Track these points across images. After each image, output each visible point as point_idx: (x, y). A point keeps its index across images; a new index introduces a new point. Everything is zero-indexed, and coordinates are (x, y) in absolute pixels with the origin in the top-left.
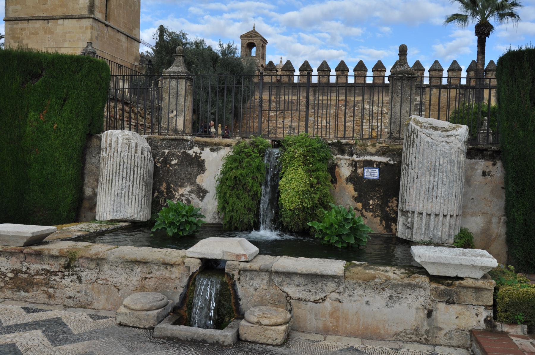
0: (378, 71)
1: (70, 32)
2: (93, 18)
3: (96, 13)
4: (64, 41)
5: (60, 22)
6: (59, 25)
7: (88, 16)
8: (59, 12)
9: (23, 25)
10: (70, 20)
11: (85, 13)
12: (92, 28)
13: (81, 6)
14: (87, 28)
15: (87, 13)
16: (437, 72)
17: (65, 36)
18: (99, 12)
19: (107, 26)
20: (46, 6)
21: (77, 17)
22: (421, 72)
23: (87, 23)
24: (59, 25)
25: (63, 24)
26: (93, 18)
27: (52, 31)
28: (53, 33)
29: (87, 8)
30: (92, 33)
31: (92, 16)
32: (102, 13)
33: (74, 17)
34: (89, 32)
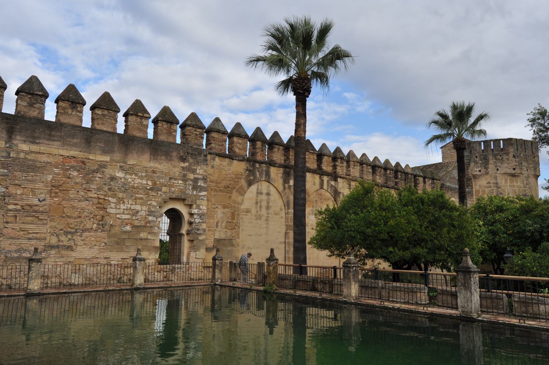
0: (137, 116)
16: (220, 135)
22: (200, 130)
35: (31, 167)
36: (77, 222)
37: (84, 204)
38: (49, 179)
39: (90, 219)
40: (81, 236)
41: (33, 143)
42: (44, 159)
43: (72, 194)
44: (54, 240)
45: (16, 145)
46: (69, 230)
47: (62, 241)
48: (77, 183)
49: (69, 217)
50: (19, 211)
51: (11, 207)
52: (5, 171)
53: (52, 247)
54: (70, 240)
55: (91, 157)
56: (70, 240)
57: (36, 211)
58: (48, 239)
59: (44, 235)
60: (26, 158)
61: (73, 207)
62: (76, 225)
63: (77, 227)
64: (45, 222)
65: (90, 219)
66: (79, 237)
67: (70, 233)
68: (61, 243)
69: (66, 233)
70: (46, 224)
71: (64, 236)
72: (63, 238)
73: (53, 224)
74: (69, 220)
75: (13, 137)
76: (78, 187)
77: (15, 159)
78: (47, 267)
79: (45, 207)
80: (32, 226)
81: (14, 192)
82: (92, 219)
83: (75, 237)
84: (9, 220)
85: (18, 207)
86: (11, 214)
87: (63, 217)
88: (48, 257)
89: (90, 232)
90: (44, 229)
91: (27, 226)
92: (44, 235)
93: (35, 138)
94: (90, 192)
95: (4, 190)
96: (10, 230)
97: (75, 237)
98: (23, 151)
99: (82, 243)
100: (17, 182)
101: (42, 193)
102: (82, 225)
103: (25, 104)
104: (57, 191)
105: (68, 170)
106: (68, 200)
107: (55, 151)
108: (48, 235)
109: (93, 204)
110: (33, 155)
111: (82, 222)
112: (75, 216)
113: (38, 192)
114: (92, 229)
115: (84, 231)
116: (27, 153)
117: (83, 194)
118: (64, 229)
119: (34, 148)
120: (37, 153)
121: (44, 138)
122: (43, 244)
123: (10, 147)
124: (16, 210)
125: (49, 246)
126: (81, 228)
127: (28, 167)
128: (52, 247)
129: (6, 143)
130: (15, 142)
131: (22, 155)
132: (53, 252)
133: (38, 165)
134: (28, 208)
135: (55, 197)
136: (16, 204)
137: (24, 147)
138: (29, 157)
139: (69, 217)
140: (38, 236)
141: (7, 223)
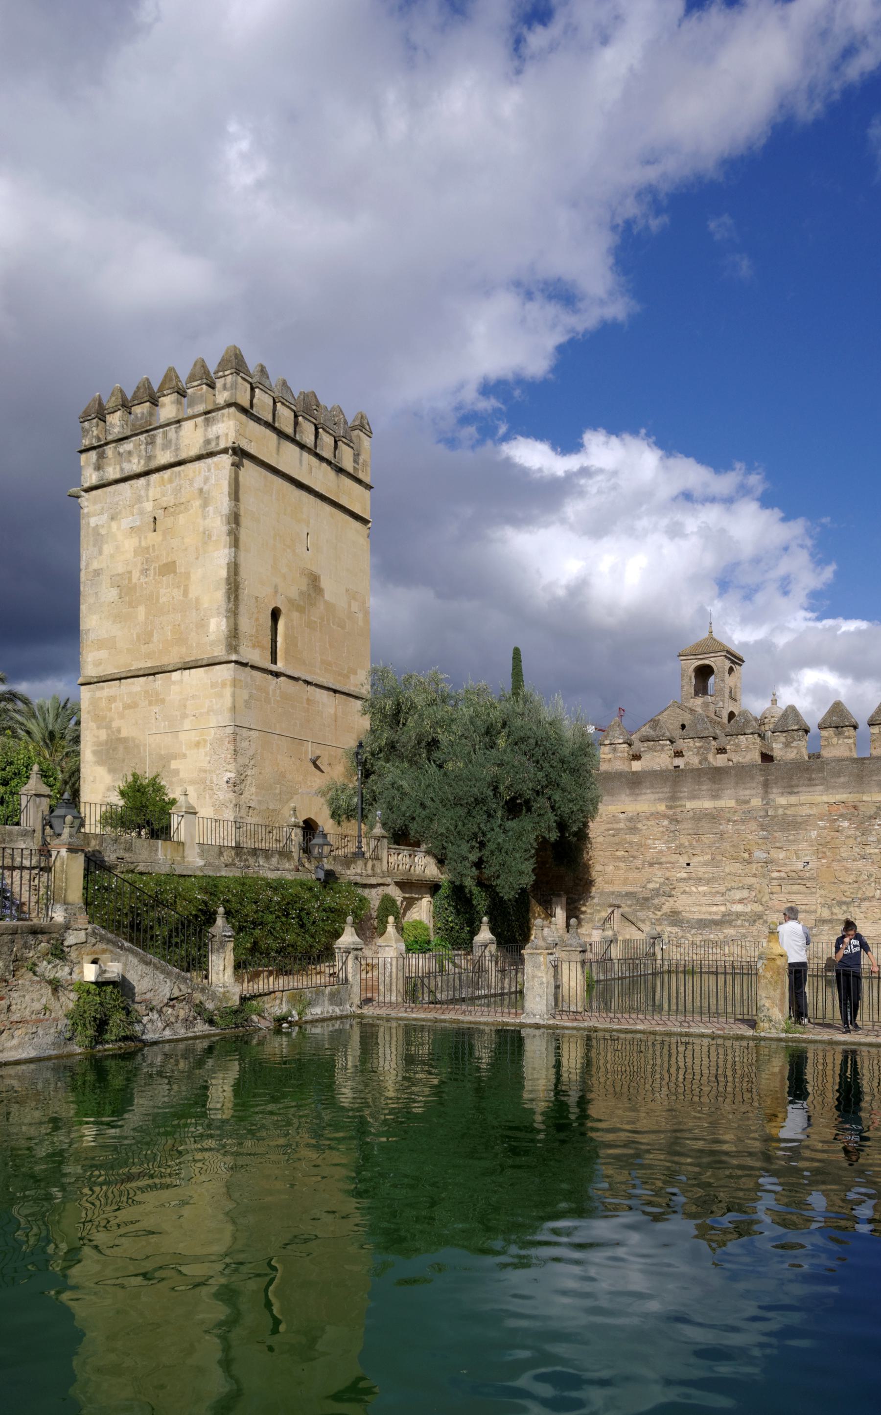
1: (193, 697)
2: (236, 662)
3: (242, 649)
4: (184, 716)
5: (176, 676)
6: (174, 683)
7: (226, 658)
8: (172, 658)
9: (109, 689)
10: (193, 671)
11: (220, 652)
12: (235, 683)
13: (213, 637)
14: (224, 685)
15: (224, 652)
17: (185, 706)
18: (254, 646)
19: (271, 673)
20: (151, 645)
21: (205, 663)
23: (225, 672)
24: (174, 683)
25: (182, 681)
26: (236, 662)
27: (161, 697)
28: (163, 701)
29: (224, 642)
30: (234, 695)
31: (234, 657)
32: (263, 648)
33: (199, 664)
34: (228, 692)
35: (793, 824)
36: (853, 888)
37: (860, 864)
38: (813, 837)
39: (869, 884)
40: (859, 907)
41: (791, 793)
42: (805, 811)
43: (844, 852)
44: (826, 914)
45: (774, 800)
46: (844, 899)
47: (836, 914)
48: (849, 837)
49: (842, 882)
50: (784, 879)
51: (775, 875)
52: (765, 833)
53: (824, 922)
54: (845, 912)
55: (865, 798)
56: (845, 912)
57: (801, 878)
58: (819, 910)
59: (814, 907)
60: (785, 814)
61: (847, 869)
62: (852, 893)
63: (852, 896)
64: (814, 890)
65: (869, 884)
66: (856, 909)
67: (844, 903)
68: (835, 917)
69: (841, 903)
70: (815, 893)
71: (837, 908)
72: (836, 910)
73: (822, 892)
74: (842, 886)
75: (769, 790)
76: (851, 842)
77: (774, 817)
78: (820, 945)
79: (812, 872)
80: (798, 897)
81: (776, 856)
82: (873, 885)
83: (851, 909)
84: (774, 890)
85: (783, 875)
86: (775, 882)
87: (835, 883)
88: (820, 934)
89: (870, 901)
90: (812, 900)
91: (794, 897)
92: (814, 907)
93: (792, 786)
94: (868, 847)
95: (765, 855)
96: (776, 902)
97: (851, 909)
98: (781, 806)
99: (862, 915)
100: (778, 845)
101: (806, 855)
102: (861, 892)
103: (781, 746)
104: (825, 850)
105: (835, 820)
106: (839, 861)
107: (818, 799)
108: (819, 906)
109: (872, 863)
110: (793, 809)
111: (860, 888)
112: (851, 881)
113: (802, 854)
114: (873, 897)
115: (862, 900)
116: (785, 808)
117: (858, 850)
118: (838, 898)
119: (793, 799)
120: (796, 805)
121: (804, 785)
122: (813, 917)
123: (767, 804)
124: (781, 878)
125: (820, 920)
126: (859, 896)
127: (789, 825)
128: (824, 922)
129: (763, 799)
130: (771, 796)
131: (780, 811)
132: (826, 928)
133: (799, 820)
134: (793, 874)
135: (823, 858)
136: (779, 871)
137: (782, 801)
138: (788, 812)
139: (842, 882)
140: (807, 908)
141: (772, 893)
